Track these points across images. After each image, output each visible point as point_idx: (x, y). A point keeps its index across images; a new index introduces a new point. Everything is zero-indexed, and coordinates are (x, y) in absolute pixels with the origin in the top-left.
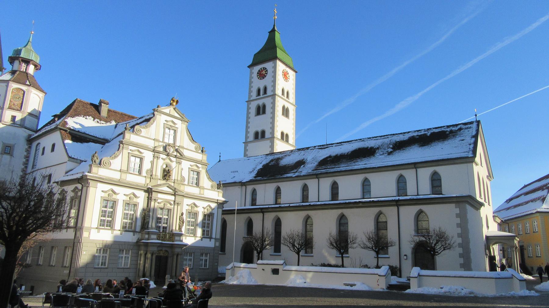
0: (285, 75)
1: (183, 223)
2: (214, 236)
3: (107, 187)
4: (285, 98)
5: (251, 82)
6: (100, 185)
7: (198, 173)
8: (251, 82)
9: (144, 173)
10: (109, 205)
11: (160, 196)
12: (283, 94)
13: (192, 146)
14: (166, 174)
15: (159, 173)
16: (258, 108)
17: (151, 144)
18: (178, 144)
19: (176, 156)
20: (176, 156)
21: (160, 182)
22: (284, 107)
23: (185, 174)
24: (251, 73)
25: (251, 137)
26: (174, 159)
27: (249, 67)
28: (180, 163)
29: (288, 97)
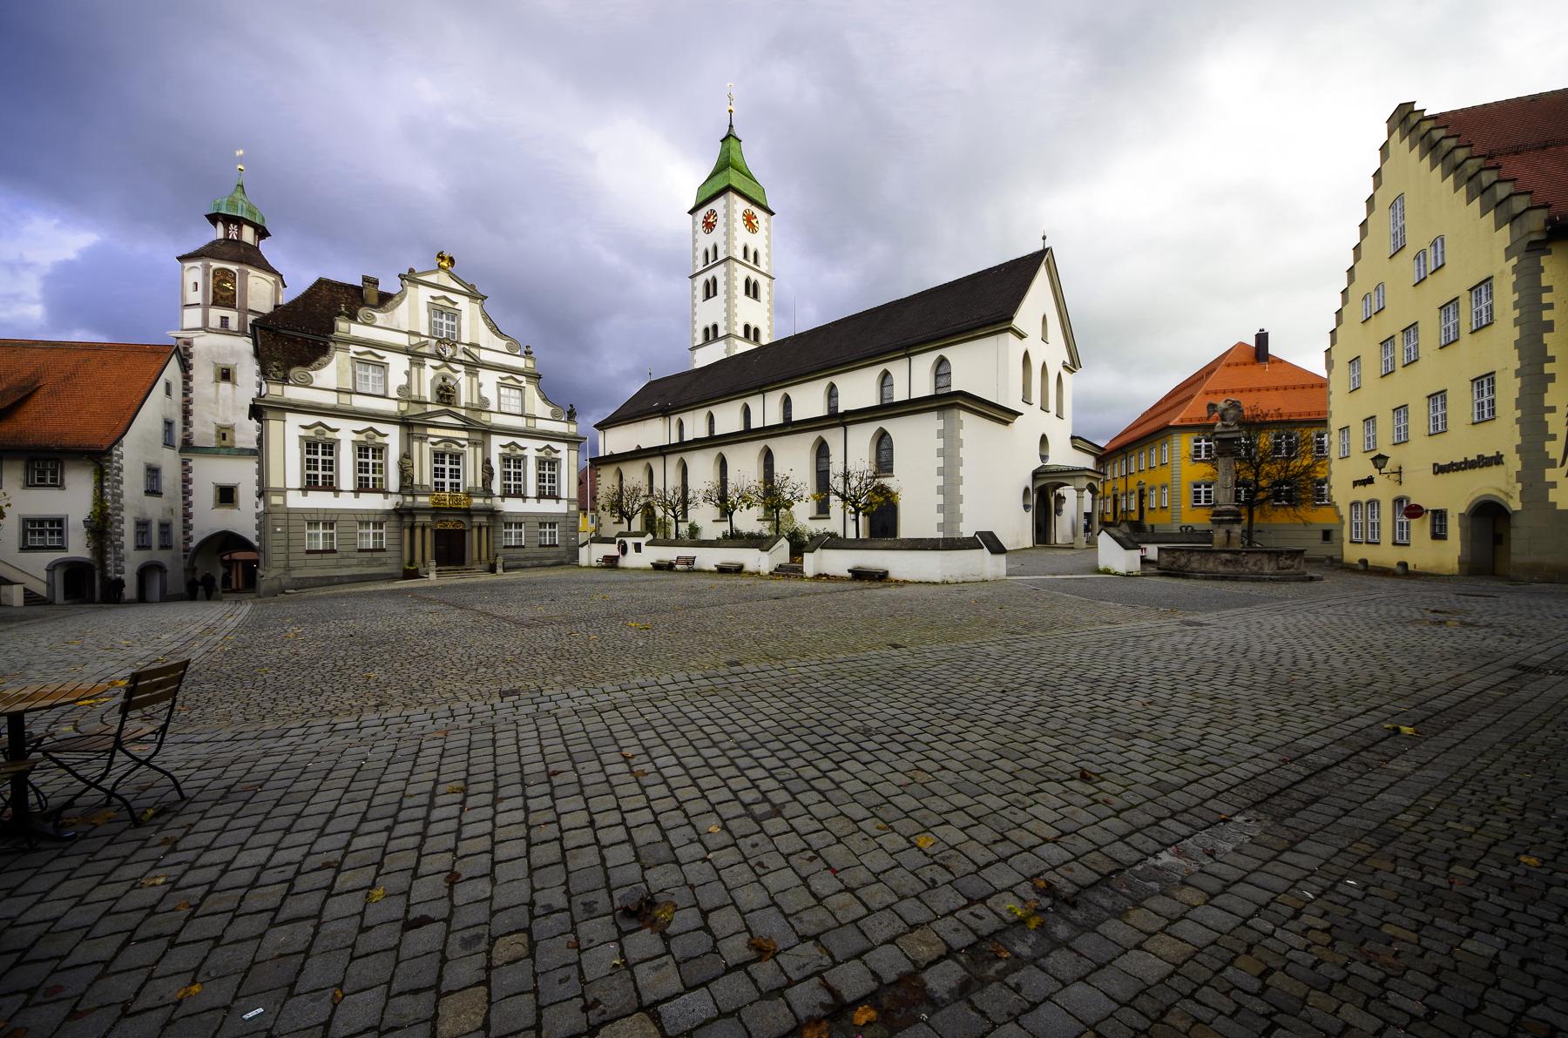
0: (749, 220)
1: (491, 474)
2: (564, 494)
3: (310, 420)
4: (751, 264)
5: (695, 241)
6: (289, 416)
7: (521, 389)
8: (695, 241)
9: (393, 393)
10: (319, 450)
11: (430, 431)
12: (745, 256)
13: (502, 344)
14: (446, 394)
15: (427, 393)
16: (707, 284)
17: (403, 340)
18: (465, 339)
19: (461, 362)
20: (461, 362)
21: (430, 408)
22: (747, 281)
23: (489, 391)
24: (694, 223)
25: (700, 339)
26: (461, 368)
27: (691, 212)
28: (476, 374)
29: (756, 261)
